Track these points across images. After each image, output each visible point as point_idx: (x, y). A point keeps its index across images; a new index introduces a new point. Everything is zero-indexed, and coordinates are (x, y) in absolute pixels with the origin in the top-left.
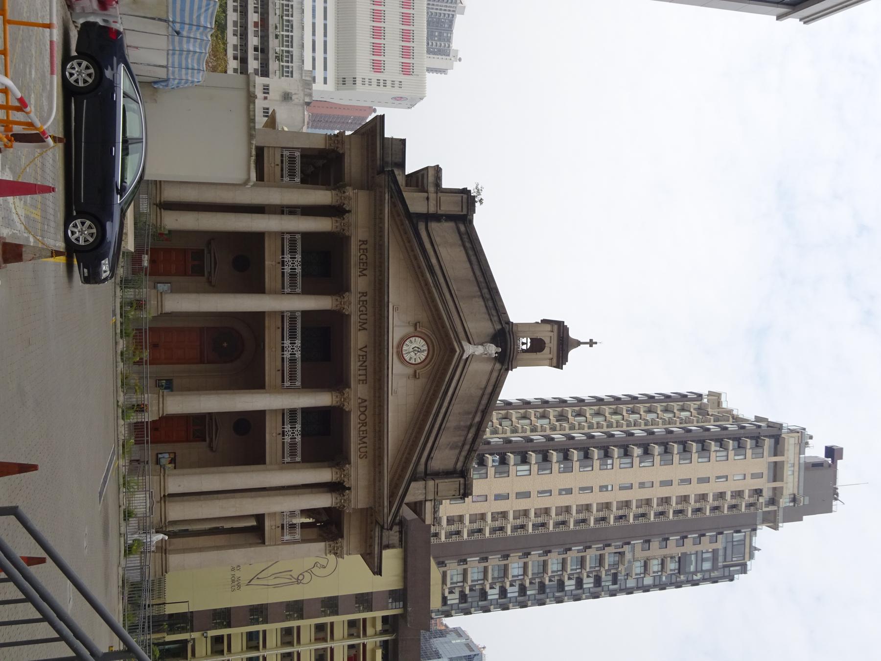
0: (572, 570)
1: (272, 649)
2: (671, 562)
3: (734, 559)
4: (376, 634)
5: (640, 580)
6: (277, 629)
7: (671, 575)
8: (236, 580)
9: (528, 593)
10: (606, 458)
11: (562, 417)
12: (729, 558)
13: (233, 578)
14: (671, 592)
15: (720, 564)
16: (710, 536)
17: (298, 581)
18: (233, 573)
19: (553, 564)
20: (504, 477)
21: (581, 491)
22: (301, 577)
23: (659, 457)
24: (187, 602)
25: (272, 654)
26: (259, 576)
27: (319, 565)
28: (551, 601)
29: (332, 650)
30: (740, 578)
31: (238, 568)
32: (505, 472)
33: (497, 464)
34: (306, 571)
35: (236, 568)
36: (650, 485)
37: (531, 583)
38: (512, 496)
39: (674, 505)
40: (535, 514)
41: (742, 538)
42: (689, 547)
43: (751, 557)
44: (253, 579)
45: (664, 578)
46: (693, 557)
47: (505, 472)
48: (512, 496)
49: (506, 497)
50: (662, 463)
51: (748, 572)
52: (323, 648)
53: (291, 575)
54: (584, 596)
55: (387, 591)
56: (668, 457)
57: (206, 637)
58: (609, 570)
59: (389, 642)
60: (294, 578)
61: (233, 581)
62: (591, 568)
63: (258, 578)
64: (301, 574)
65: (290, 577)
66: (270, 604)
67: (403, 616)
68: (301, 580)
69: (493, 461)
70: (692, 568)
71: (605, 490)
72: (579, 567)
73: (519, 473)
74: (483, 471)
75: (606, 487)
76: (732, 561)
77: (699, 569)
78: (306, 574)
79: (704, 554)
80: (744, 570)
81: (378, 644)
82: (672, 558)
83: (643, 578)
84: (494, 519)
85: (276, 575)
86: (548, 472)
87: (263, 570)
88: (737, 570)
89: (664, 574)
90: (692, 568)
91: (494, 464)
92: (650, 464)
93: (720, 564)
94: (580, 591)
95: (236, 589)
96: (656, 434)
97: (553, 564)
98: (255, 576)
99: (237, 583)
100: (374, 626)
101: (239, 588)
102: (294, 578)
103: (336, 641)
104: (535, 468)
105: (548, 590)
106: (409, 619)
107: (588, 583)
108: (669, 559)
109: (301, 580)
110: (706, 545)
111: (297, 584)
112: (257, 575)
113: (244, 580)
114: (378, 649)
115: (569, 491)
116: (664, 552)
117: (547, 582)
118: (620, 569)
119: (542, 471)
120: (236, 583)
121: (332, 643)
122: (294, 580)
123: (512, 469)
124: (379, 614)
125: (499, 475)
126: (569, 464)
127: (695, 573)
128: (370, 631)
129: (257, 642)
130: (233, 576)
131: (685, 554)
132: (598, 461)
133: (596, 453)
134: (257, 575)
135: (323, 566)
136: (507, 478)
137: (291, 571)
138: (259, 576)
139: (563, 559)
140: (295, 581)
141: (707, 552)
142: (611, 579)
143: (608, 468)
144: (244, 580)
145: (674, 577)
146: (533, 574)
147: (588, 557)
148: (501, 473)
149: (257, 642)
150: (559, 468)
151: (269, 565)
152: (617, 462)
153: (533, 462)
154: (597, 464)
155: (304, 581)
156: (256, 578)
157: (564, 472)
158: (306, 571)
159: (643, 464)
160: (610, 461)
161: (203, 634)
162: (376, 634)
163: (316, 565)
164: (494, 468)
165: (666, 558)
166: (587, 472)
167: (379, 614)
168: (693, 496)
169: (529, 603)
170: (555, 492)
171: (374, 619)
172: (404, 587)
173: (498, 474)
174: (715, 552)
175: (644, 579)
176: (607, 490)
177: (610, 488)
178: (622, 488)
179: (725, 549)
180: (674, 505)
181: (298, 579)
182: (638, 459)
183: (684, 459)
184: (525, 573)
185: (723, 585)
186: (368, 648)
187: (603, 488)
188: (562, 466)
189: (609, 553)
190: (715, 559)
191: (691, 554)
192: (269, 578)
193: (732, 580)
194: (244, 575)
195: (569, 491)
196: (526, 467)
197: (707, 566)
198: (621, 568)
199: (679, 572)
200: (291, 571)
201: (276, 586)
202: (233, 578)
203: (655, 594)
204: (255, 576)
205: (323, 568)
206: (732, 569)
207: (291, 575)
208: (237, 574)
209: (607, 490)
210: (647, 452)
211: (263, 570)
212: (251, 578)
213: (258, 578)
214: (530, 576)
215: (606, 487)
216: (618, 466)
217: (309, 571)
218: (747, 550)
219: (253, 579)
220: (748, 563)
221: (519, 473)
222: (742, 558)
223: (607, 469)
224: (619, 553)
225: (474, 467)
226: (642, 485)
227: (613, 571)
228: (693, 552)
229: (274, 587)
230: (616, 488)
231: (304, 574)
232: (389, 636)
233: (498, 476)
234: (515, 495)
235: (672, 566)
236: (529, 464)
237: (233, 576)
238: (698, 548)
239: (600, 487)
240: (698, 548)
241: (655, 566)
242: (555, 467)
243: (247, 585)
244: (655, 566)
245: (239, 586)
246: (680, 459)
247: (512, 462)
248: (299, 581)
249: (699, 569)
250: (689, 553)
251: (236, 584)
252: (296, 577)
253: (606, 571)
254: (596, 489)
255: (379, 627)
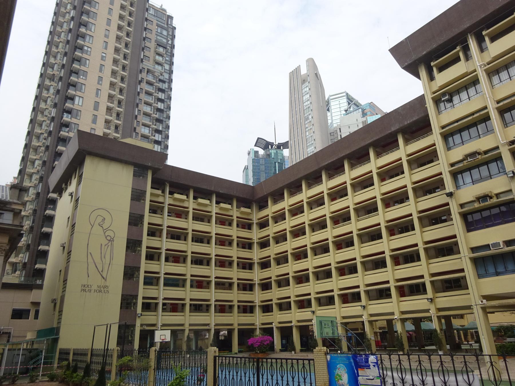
0: (152, 100)
1: (161, 268)
2: (159, 49)
3: (164, 19)
4: (164, 196)
5: (166, 71)
6: (145, 263)
7: (166, 54)
8: (99, 289)
9: (161, 129)
10: (83, 49)
11: (52, 78)
12: (163, 22)
13: (98, 291)
14: (175, 60)
15: (166, 26)
16: (147, 15)
17: (111, 240)
18: (93, 291)
19: (148, 109)
20: (81, 114)
21: (102, 71)
22: (109, 238)
23: (90, 19)
24: (95, 328)
25: (164, 268)
26: (100, 270)
27: (102, 223)
28: (168, 121)
29: (168, 227)
30: (175, 23)
31: (90, 286)
32: (77, 113)
33: (70, 116)
34: (105, 233)
35: (89, 289)
36: (107, 32)
37: (155, 125)
38: (96, 113)
39: (124, 24)
40: (111, 103)
41: (153, 10)
42: (153, 36)
43: (165, 11)
44: (101, 275)
45: (167, 59)
46: (158, 38)
47: (77, 113)
48: (96, 113)
49: (95, 116)
50: (94, 19)
51: (173, 16)
52: (167, 234)
53: (105, 245)
54: (169, 103)
55: (133, 178)
56: (91, 14)
57: (141, 315)
58: (156, 81)
59: (171, 190)
60: (108, 243)
61: (100, 291)
62: (153, 90)
63: (102, 271)
64: (106, 238)
65: (106, 247)
66: (125, 263)
67: (155, 171)
68: (111, 238)
69: (67, 117)
70: (165, 41)
71: (104, 58)
72: (151, 96)
73: (80, 104)
74: (73, 126)
75: (102, 57)
76: (165, 21)
77: (166, 37)
78: (106, 234)
79: (158, 31)
80: (170, 18)
81: (170, 196)
82: (157, 48)
83: (165, 69)
84: (109, 128)
85: (102, 257)
86: (83, 87)
87: (96, 267)
88: (171, 22)
89: (165, 56)
90: (165, 41)
91: (70, 117)
92: (93, 26)
93: (166, 26)
94: (166, 103)
95: (107, 289)
96: (74, 16)
97: (146, 110)
98: (100, 273)
99: (102, 288)
100: (158, 196)
101: (107, 287)
102: (108, 243)
103: (163, 223)
104: (78, 93)
105: (161, 118)
106: (156, 167)
107: (161, 96)
108: (157, 50)
109: (111, 238)
110: (154, 27)
111: (113, 241)
112: (99, 272)
113: (100, 282)
114: (174, 196)
115: (100, 79)
116: (152, 50)
117: (157, 116)
118: (157, 75)
119: (82, 89)
120: (102, 289)
121: (164, 226)
122: (110, 244)
123: (76, 107)
124: (149, 190)
125: (78, 116)
126: (81, 73)
127: (168, 41)
128: (161, 199)
129: (154, 279)
130: (95, 291)
131: (156, 41)
132: (84, 54)
133: (78, 53)
134: (99, 272)
135: (103, 220)
136: (82, 112)
137: (101, 245)
138: (100, 270)
139: (145, 103)
140: (111, 242)
141: (157, 29)
142: (162, 83)
143: (90, 50)
144: (100, 282)
145: (167, 53)
146: (150, 122)
147: (146, 89)
148: (77, 115)
149: (154, 279)
150: (83, 79)
151: (92, 261)
152: (86, 44)
153: (74, 93)
154: (85, 56)
155: (112, 236)
156: (101, 273)
157: (86, 77)
158: (105, 233)
159: (93, 30)
160: (86, 48)
161: (139, 317)
162: (164, 196)
163: (100, 225)
164: (73, 119)
165: (156, 51)
166: (90, 63)
167: (149, 190)
168: (120, 11)
169: (167, 132)
170: (99, 87)
171: (152, 194)
172: (133, 165)
173: (77, 117)
174: (158, 25)
175: (165, 68)
176: (105, 57)
177: (104, 55)
178: (106, 48)
179: (157, 20)
180: (124, 24)
181: (110, 240)
182: (88, 31)
183: (95, 6)
184: (148, 126)
185: (177, 33)
186: (172, 202)
187: (103, 58)
188: (82, 77)
189: (147, 77)
190: (162, 28)
191: (157, 38)
192: (104, 263)
193: (175, 28)
194: (96, 281)
195: (100, 79)
196: (77, 99)
197: (165, 33)
198: (156, 74)
199: (166, 48)
200: (101, 245)
201: (111, 258)
202: (98, 291)
203: (175, 68)
204: (100, 273)
205: (104, 220)
206: (169, 23)
207: (105, 245)
208: (95, 287)
209: (105, 57)
210: (85, 25)
211: (96, 267)
212: (101, 277)
213: (102, 271)
214: (151, 123)
215: (102, 57)
216: (90, 44)
217: (105, 231)
218: (161, 11)
219: (101, 275)
220: (168, 14)
221: (80, 104)
222: (165, 15)
223: (90, 52)
224: (148, 72)
225: (68, 130)
226: (106, 36)
227: (158, 80)
228: (156, 37)
229: (112, 259)
230: (105, 51)
231: (106, 235)
232: (167, 187)
233: (79, 118)
234: (95, 111)
235: (161, 50)
236: (75, 96)
237: (95, 291)
238: (154, 32)
239: (101, 60)
240: (154, 32)
241: (159, 59)
242: (81, 81)
243: (106, 280)
244: (159, 59)
245: (106, 287)
246: (95, 8)
247: (71, 106)
248: (112, 240)
249: (166, 37)
250: (156, 39)
251: (103, 289)
252: (108, 242)
253: (156, 82)
254: (103, 63)
255: (159, 192)
